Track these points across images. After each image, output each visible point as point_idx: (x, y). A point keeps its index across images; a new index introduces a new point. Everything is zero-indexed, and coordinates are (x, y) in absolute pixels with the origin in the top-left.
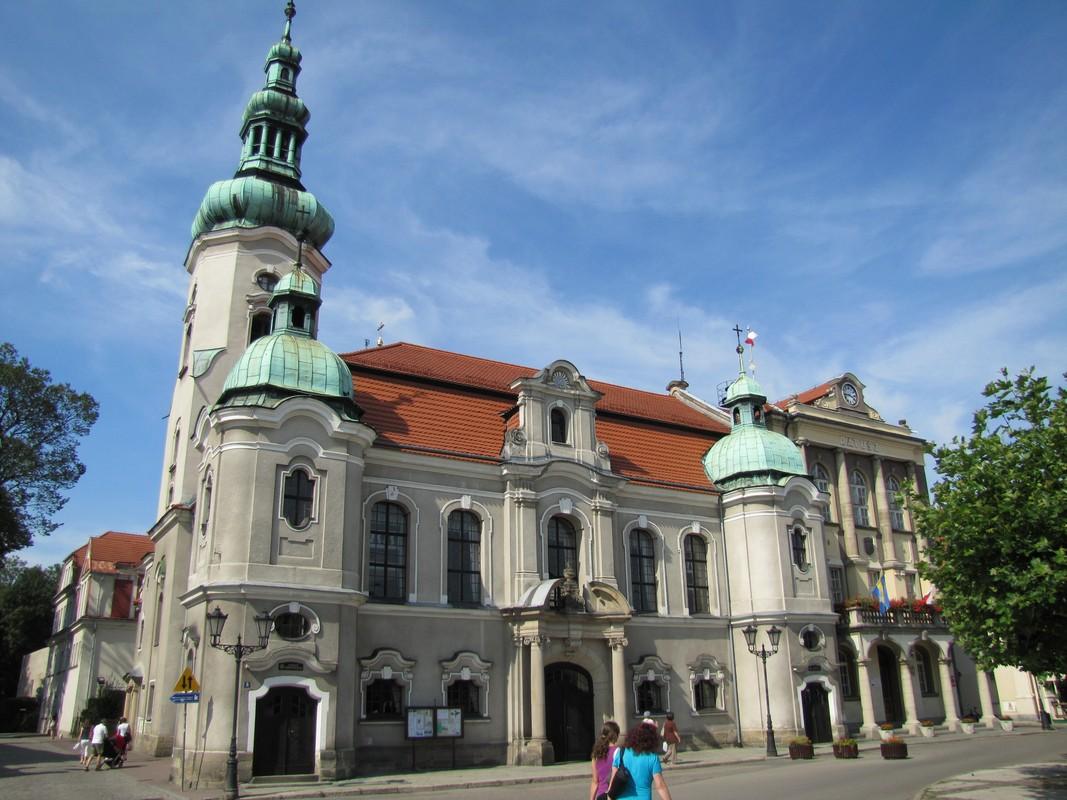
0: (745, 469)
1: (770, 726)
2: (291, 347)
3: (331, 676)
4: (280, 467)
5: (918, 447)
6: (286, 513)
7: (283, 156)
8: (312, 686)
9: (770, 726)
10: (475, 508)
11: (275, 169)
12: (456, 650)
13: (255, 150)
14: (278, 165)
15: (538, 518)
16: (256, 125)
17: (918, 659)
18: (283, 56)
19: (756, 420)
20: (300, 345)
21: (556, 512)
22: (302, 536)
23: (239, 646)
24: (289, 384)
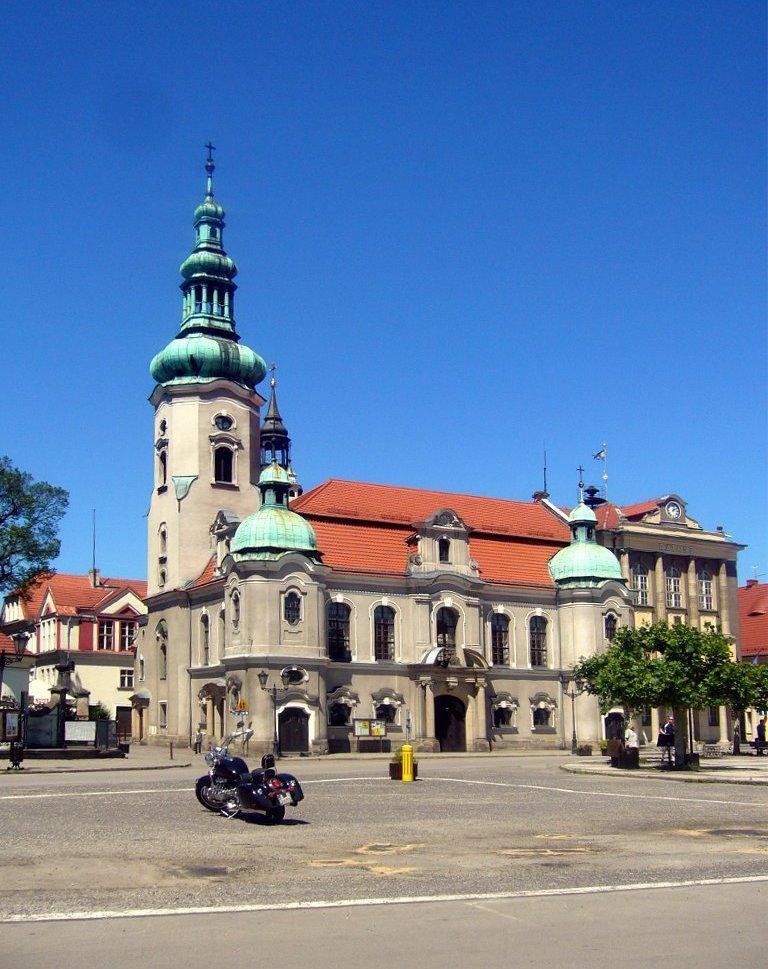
0: (575, 575)
3: (314, 703)
4: (281, 592)
10: (391, 605)
15: (431, 610)
19: (589, 536)
21: (442, 606)
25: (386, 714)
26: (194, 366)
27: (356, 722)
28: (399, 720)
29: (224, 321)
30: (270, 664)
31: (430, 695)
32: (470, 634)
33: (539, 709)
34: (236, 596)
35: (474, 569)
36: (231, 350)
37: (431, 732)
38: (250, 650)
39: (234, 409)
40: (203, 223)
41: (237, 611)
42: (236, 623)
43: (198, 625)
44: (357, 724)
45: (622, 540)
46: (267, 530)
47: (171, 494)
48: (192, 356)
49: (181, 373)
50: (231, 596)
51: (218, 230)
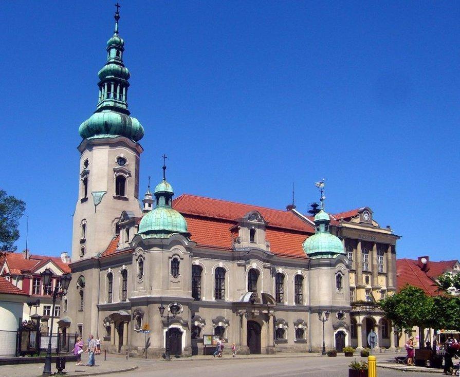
1: (324, 345)
2: (169, 215)
3: (185, 325)
4: (170, 258)
5: (394, 238)
6: (172, 273)
7: (121, 98)
8: (182, 329)
9: (324, 345)
13: (108, 97)
14: (119, 103)
17: (383, 324)
18: (117, 44)
21: (251, 268)
22: (176, 280)
25: (219, 331)
26: (106, 127)
27: (205, 337)
28: (226, 335)
29: (122, 104)
30: (162, 301)
31: (245, 320)
32: (266, 285)
33: (299, 329)
34: (141, 260)
35: (268, 246)
36: (127, 119)
37: (245, 343)
38: (150, 293)
39: (128, 154)
40: (113, 48)
41: (141, 269)
42: (141, 276)
43: (106, 279)
44: (206, 338)
45: (341, 232)
46: (162, 220)
47: (91, 202)
48: (106, 122)
49: (98, 133)
50: (137, 260)
51: (120, 52)
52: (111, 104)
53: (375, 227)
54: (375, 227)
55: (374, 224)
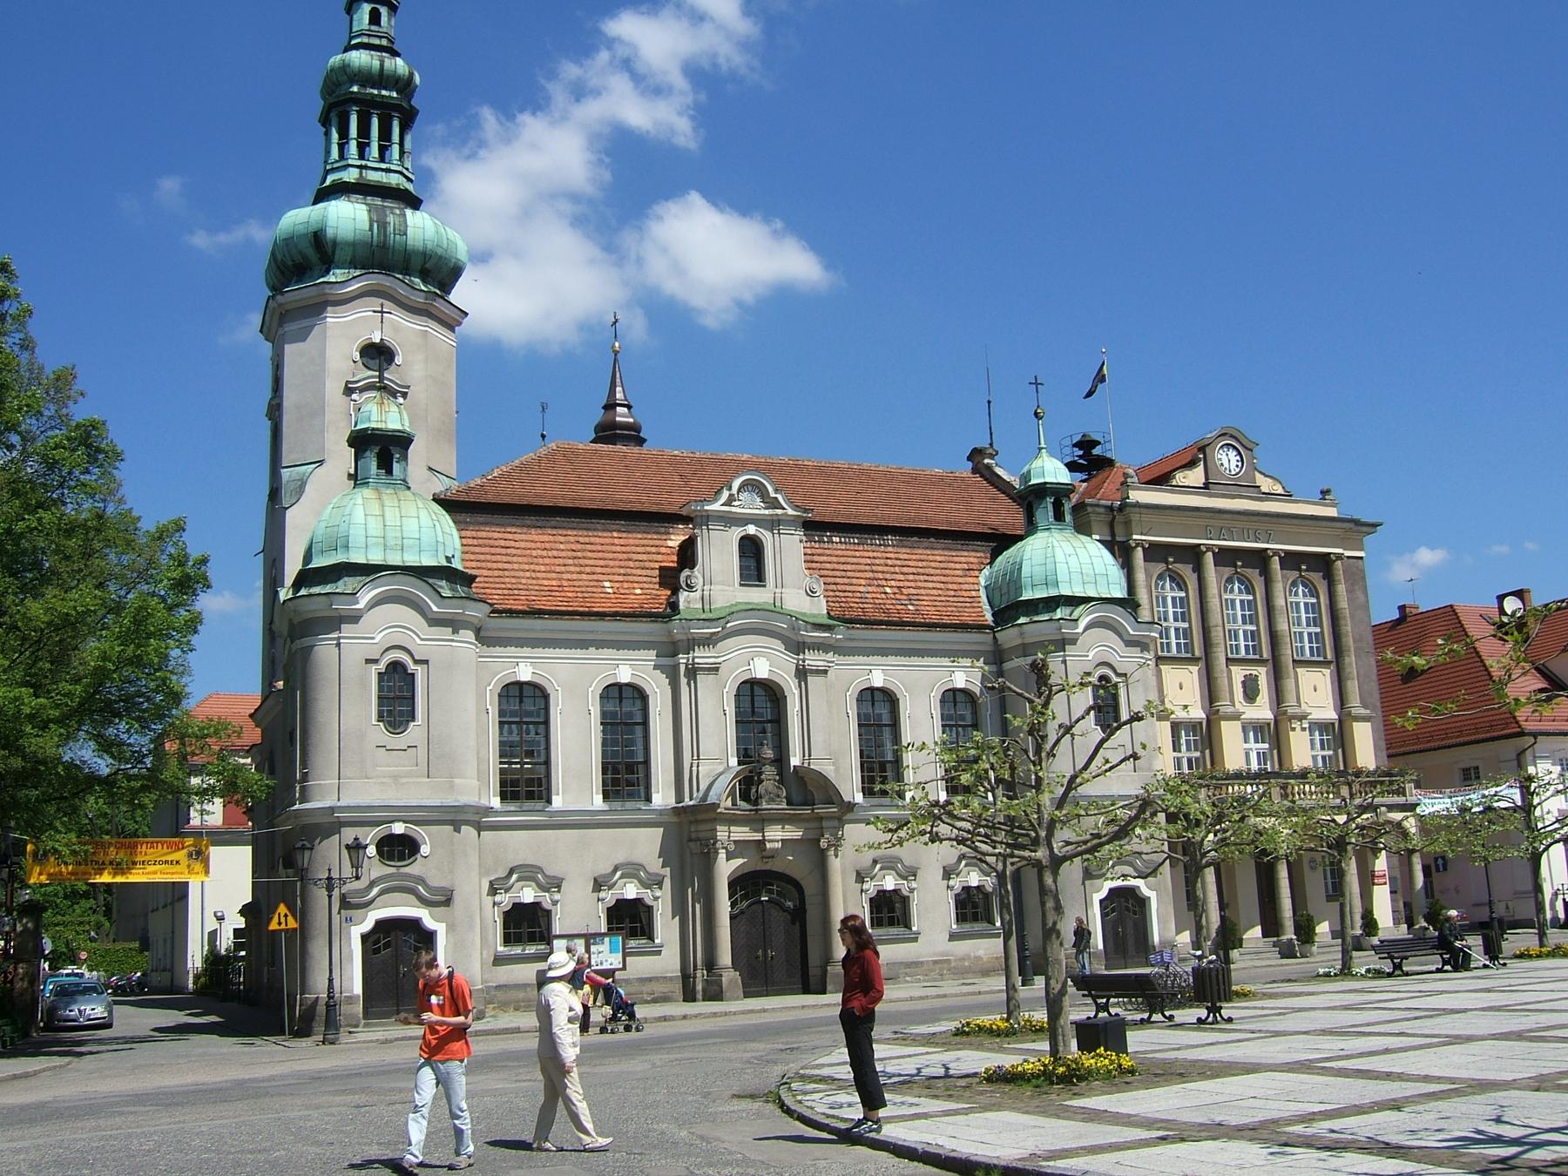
2: (375, 508)
11: (373, 176)
12: (617, 862)
16: (341, 109)
20: (387, 503)
21: (747, 677)
22: (401, 741)
23: (329, 879)
24: (376, 558)
45: (1127, 524)
52: (351, 176)
53: (1269, 496)
54: (1269, 496)
55: (1266, 484)
